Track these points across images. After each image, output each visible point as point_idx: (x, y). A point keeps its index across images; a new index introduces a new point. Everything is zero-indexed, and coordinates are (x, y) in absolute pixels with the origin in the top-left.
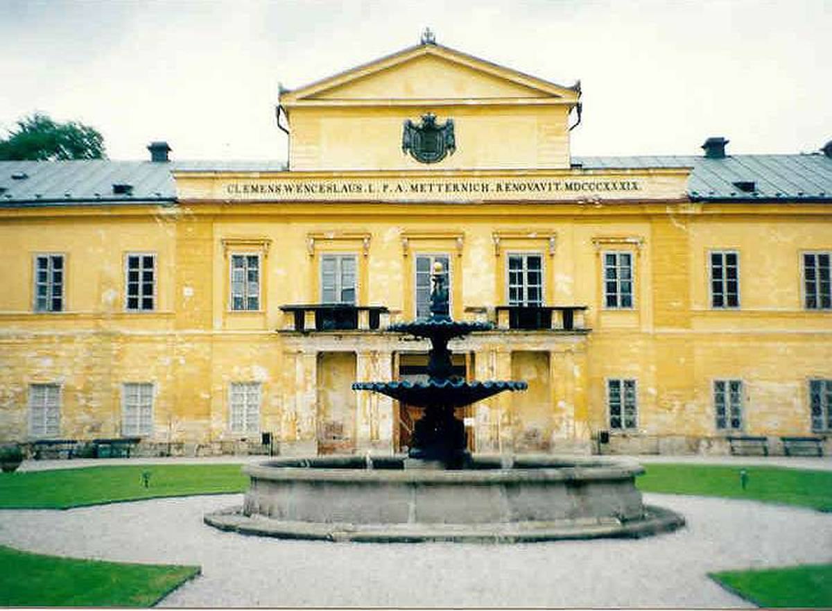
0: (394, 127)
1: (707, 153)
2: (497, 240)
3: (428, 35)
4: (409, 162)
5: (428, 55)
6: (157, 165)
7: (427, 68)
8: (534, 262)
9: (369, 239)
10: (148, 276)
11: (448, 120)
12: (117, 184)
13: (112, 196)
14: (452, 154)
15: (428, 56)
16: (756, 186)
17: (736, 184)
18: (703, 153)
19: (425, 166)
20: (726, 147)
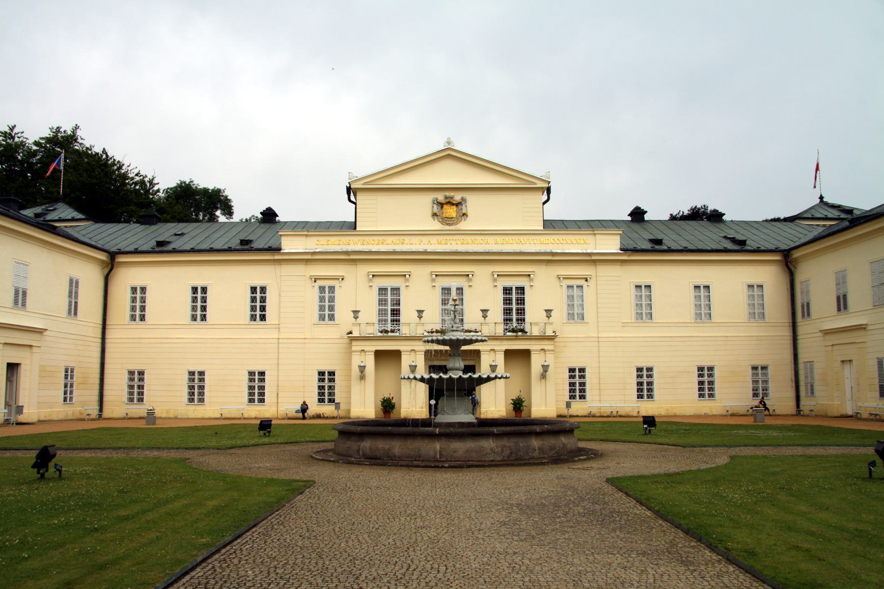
0: (426, 202)
1: (632, 219)
2: (496, 276)
3: (449, 143)
4: (436, 225)
5: (449, 155)
6: (267, 226)
7: (448, 164)
8: (521, 290)
9: (410, 275)
10: (263, 300)
11: (462, 197)
12: (241, 239)
13: (239, 247)
14: (465, 220)
15: (449, 156)
16: (663, 241)
17: (651, 241)
18: (629, 218)
19: (447, 228)
20: (645, 215)
